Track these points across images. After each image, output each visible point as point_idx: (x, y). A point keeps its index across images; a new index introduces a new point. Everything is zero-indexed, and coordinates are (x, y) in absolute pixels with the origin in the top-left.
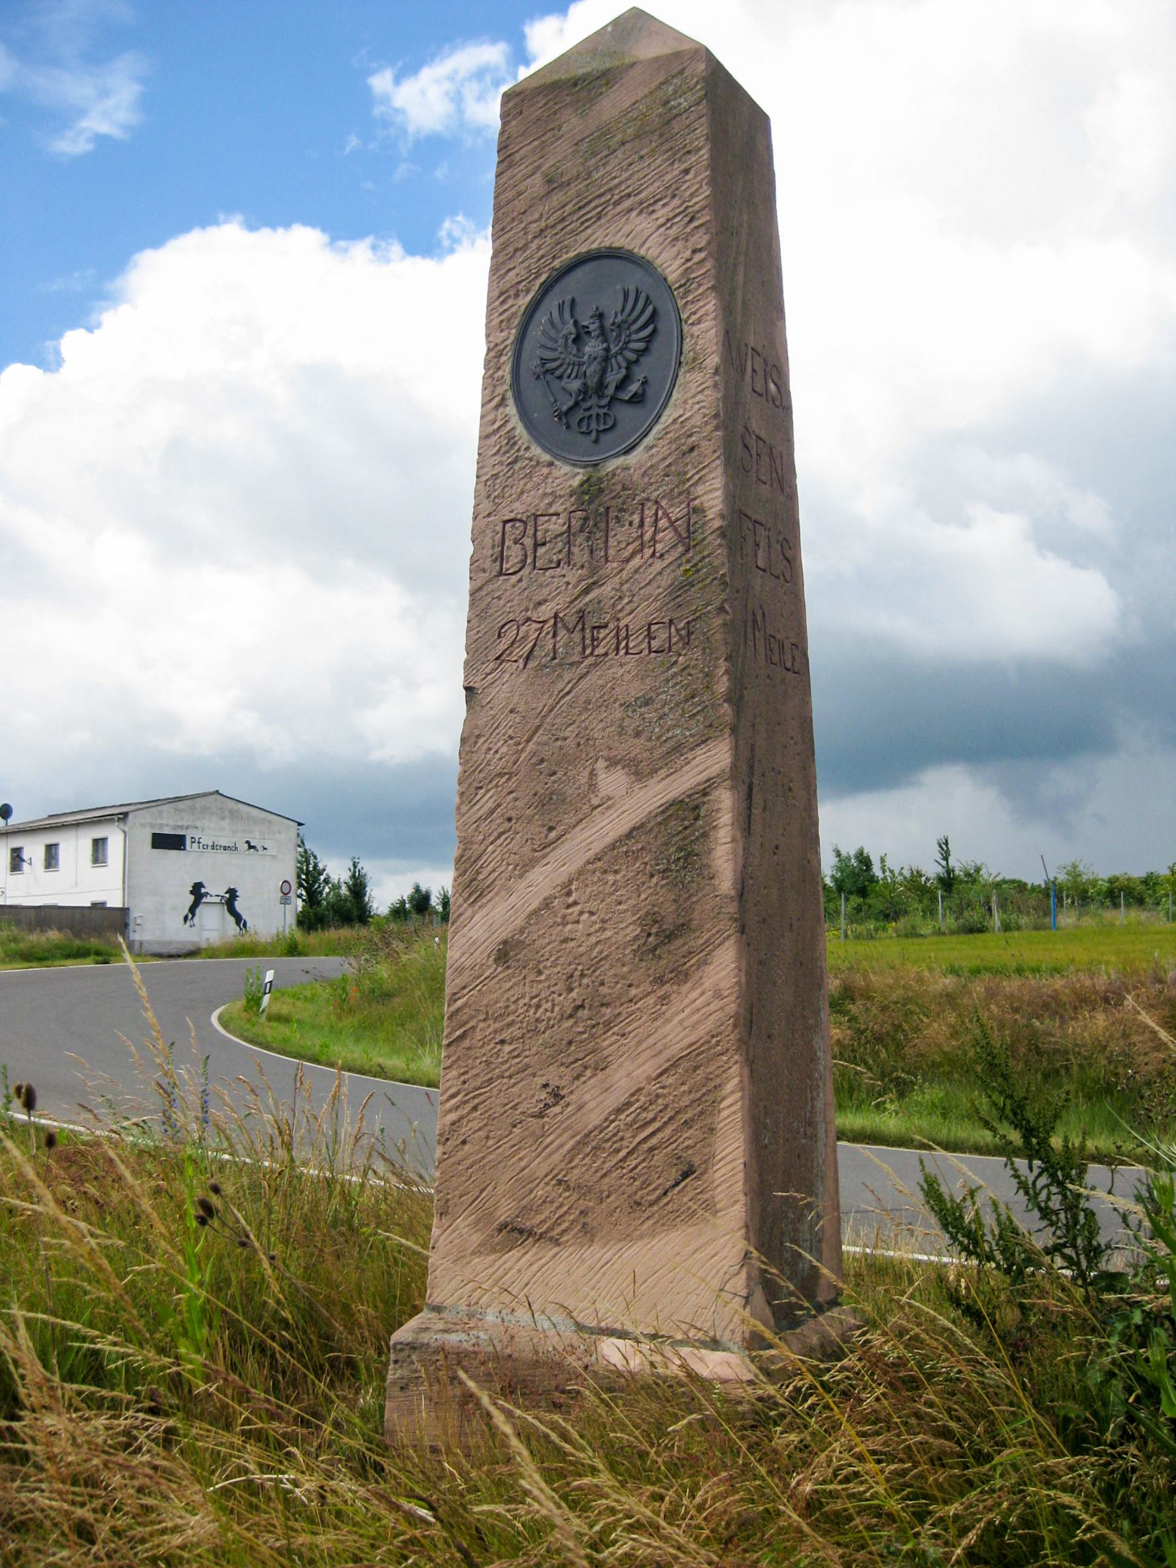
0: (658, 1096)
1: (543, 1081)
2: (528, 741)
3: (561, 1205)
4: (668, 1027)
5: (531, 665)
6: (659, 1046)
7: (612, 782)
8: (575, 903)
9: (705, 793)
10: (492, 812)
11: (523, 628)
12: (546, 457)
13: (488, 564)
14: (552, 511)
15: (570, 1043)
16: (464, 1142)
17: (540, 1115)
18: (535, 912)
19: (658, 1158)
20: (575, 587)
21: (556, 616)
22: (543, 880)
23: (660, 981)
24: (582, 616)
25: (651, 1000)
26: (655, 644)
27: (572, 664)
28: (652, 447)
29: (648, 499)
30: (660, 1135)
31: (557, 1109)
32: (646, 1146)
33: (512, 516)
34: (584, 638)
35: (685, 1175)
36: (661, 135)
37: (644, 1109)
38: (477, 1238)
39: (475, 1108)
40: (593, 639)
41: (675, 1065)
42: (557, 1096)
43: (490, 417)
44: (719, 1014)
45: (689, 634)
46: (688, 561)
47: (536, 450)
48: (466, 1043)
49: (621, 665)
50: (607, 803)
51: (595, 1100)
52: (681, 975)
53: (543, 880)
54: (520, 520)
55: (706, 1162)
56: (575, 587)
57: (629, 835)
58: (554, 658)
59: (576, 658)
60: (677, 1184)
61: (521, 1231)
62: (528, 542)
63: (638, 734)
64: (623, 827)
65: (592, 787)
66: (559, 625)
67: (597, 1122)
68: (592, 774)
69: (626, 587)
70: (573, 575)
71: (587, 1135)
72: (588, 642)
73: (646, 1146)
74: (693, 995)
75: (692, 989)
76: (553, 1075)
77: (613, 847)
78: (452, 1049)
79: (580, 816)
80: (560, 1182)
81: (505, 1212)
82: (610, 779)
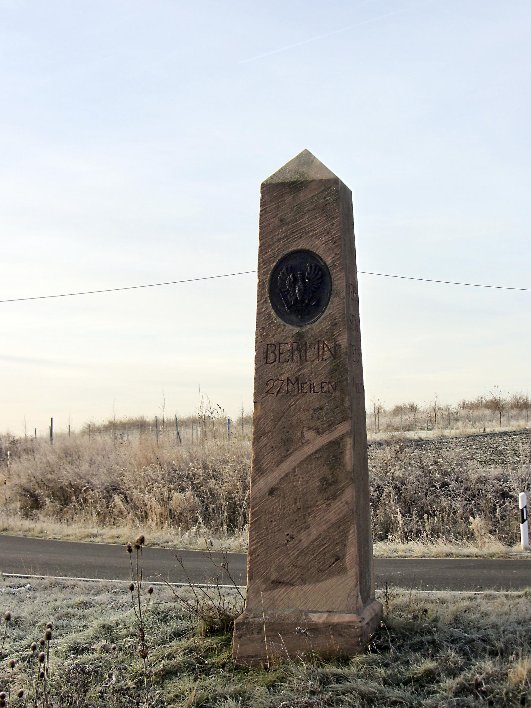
0: (327, 536)
1: (287, 533)
2: (279, 421)
3: (294, 573)
4: (330, 514)
5: (279, 395)
6: (327, 520)
7: (309, 435)
8: (297, 475)
9: (342, 439)
10: (266, 445)
11: (276, 382)
12: (283, 323)
13: (262, 359)
14: (286, 342)
15: (296, 521)
16: (258, 555)
17: (286, 545)
18: (282, 478)
19: (328, 555)
20: (295, 369)
21: (288, 378)
22: (285, 467)
23: (328, 499)
24: (297, 379)
25: (324, 506)
26: (324, 390)
27: (294, 395)
28: (321, 322)
29: (320, 340)
30: (328, 548)
31: (292, 542)
32: (323, 552)
33: (270, 343)
34: (298, 387)
35: (337, 560)
36: (323, 210)
37: (322, 540)
38: (264, 586)
39: (262, 544)
40: (302, 387)
41: (333, 526)
42: (292, 538)
43: (261, 306)
44: (347, 509)
45: (336, 387)
46: (335, 362)
47: (279, 320)
48: (259, 522)
49: (312, 396)
50: (308, 442)
51: (305, 539)
52: (335, 497)
53: (285, 467)
54: (273, 344)
55: (343, 555)
56: (295, 369)
57: (316, 452)
58: (288, 393)
59: (296, 393)
60: (334, 563)
61: (280, 583)
62: (277, 353)
63: (318, 419)
64: (314, 450)
65: (302, 436)
66: (289, 382)
67: (306, 545)
68: (302, 432)
69: (313, 370)
70: (294, 365)
71: (302, 550)
72: (300, 388)
73: (323, 552)
74: (339, 503)
75: (338, 501)
76: (290, 532)
77: (310, 456)
78: (253, 525)
79: (298, 446)
80: (294, 565)
81: (273, 578)
82: (309, 434)
